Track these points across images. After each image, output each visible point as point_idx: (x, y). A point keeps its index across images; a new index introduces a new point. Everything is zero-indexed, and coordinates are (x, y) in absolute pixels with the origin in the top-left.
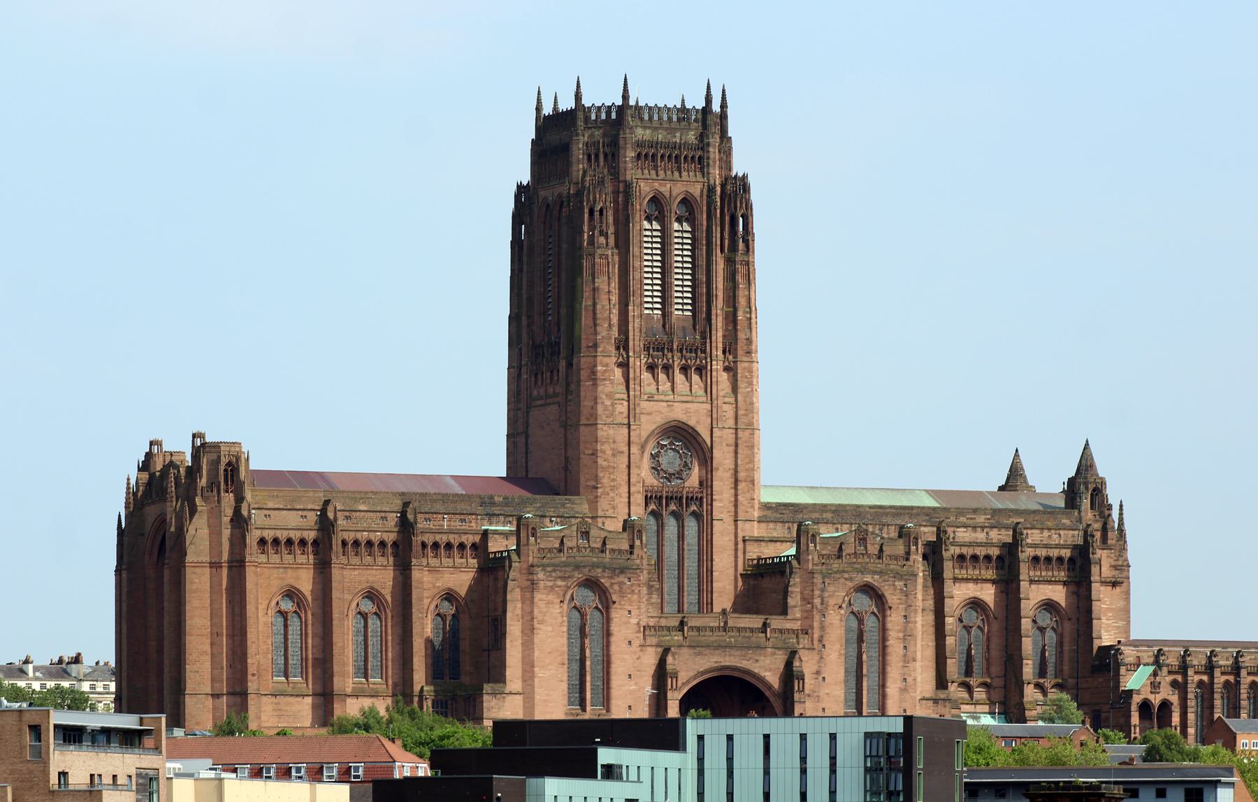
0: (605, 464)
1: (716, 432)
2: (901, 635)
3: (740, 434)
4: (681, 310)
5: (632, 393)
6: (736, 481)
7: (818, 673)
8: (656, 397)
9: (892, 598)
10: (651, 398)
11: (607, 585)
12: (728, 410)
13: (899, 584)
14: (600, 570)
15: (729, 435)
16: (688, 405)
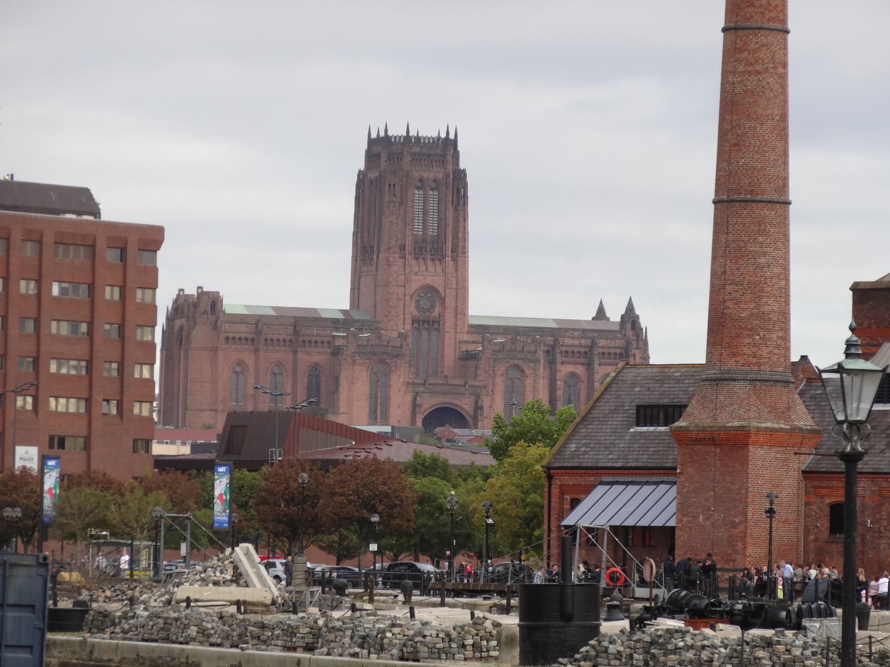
0: (392, 304)
1: (447, 291)
2: (532, 389)
3: (459, 291)
4: (432, 231)
5: (406, 271)
6: (456, 314)
7: (491, 407)
8: (418, 273)
9: (528, 372)
10: (416, 274)
11: (389, 363)
12: (454, 281)
13: (532, 365)
14: (386, 356)
15: (453, 292)
16: (434, 277)
